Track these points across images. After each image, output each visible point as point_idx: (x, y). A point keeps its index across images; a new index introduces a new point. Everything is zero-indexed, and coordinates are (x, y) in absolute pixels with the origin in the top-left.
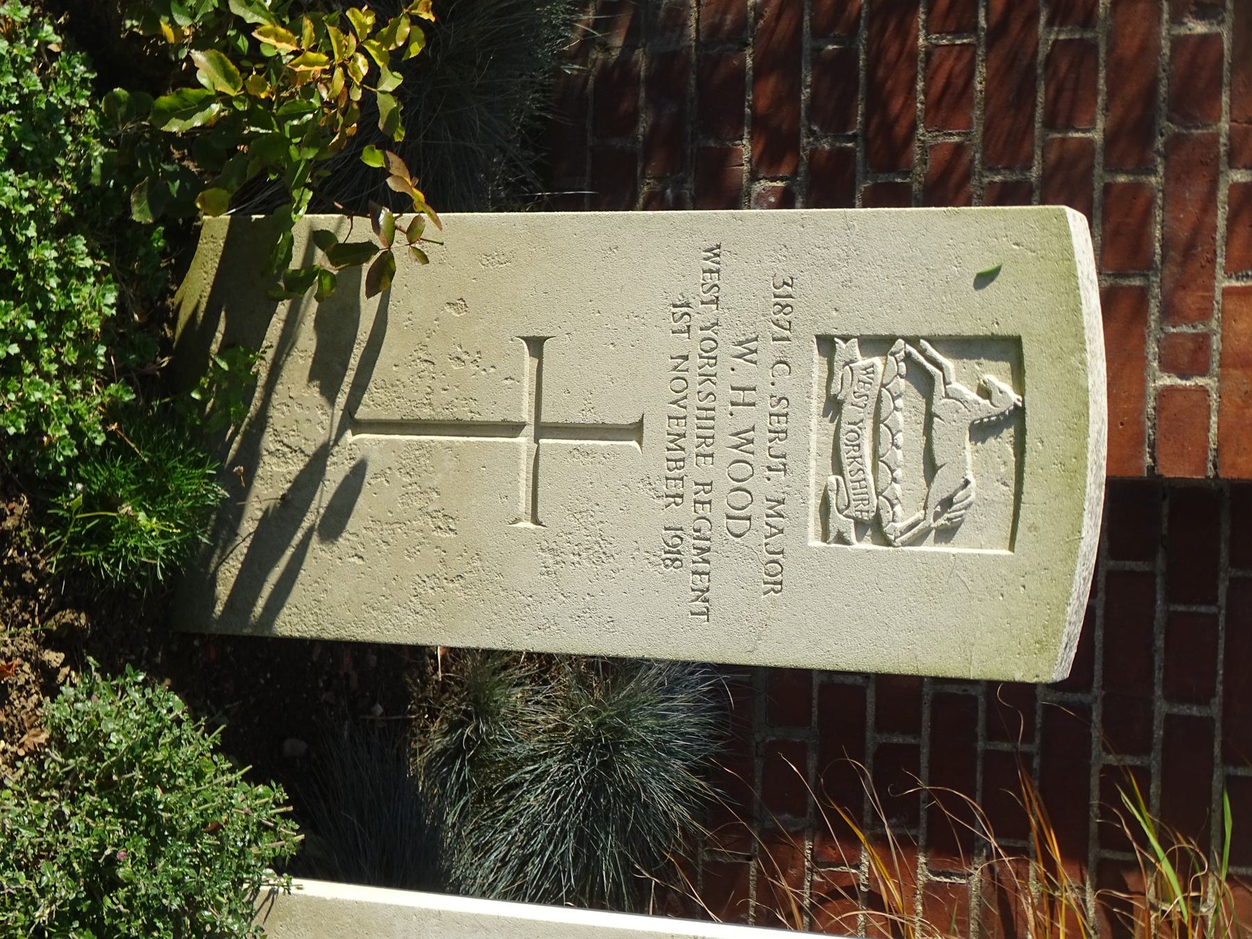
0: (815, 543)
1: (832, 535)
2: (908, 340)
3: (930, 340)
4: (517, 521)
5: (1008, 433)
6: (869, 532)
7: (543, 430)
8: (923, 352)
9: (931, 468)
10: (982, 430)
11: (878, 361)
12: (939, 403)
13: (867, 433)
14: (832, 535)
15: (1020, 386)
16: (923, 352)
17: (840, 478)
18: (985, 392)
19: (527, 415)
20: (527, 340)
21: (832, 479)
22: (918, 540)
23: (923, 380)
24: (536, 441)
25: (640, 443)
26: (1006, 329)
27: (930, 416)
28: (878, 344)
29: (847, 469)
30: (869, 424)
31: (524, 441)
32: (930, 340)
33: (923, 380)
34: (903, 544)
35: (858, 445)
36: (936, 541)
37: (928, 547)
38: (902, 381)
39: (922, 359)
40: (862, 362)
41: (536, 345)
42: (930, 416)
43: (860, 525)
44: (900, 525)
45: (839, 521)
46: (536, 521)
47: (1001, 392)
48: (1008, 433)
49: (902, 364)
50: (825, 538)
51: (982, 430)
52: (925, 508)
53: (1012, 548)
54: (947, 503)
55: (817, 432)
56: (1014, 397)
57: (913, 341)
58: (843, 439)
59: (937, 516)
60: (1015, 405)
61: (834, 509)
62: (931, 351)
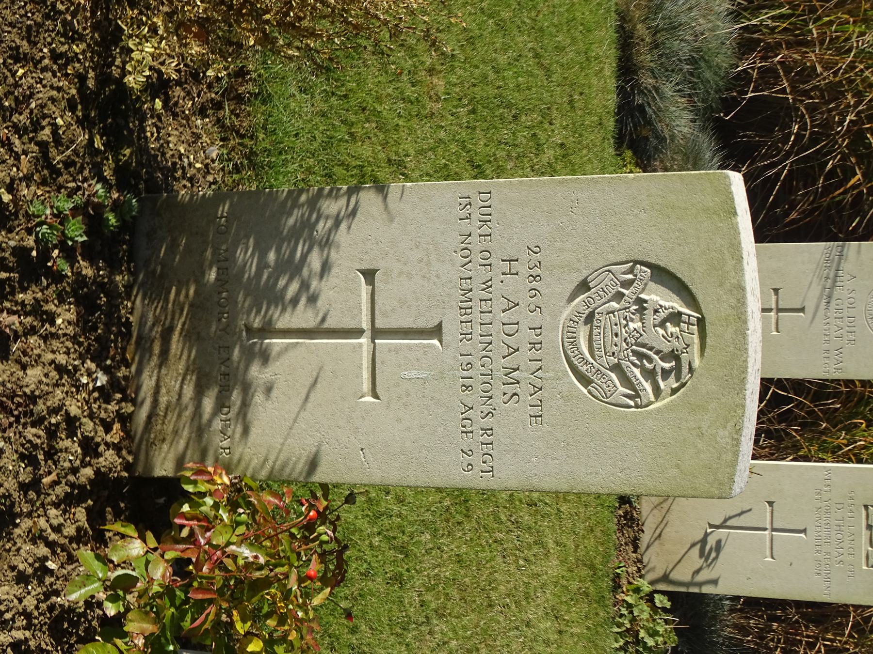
7: (774, 530)
14: (870, 565)
21: (870, 549)
25: (806, 535)
31: (766, 532)
41: (771, 503)
46: (772, 557)
50: (867, 566)
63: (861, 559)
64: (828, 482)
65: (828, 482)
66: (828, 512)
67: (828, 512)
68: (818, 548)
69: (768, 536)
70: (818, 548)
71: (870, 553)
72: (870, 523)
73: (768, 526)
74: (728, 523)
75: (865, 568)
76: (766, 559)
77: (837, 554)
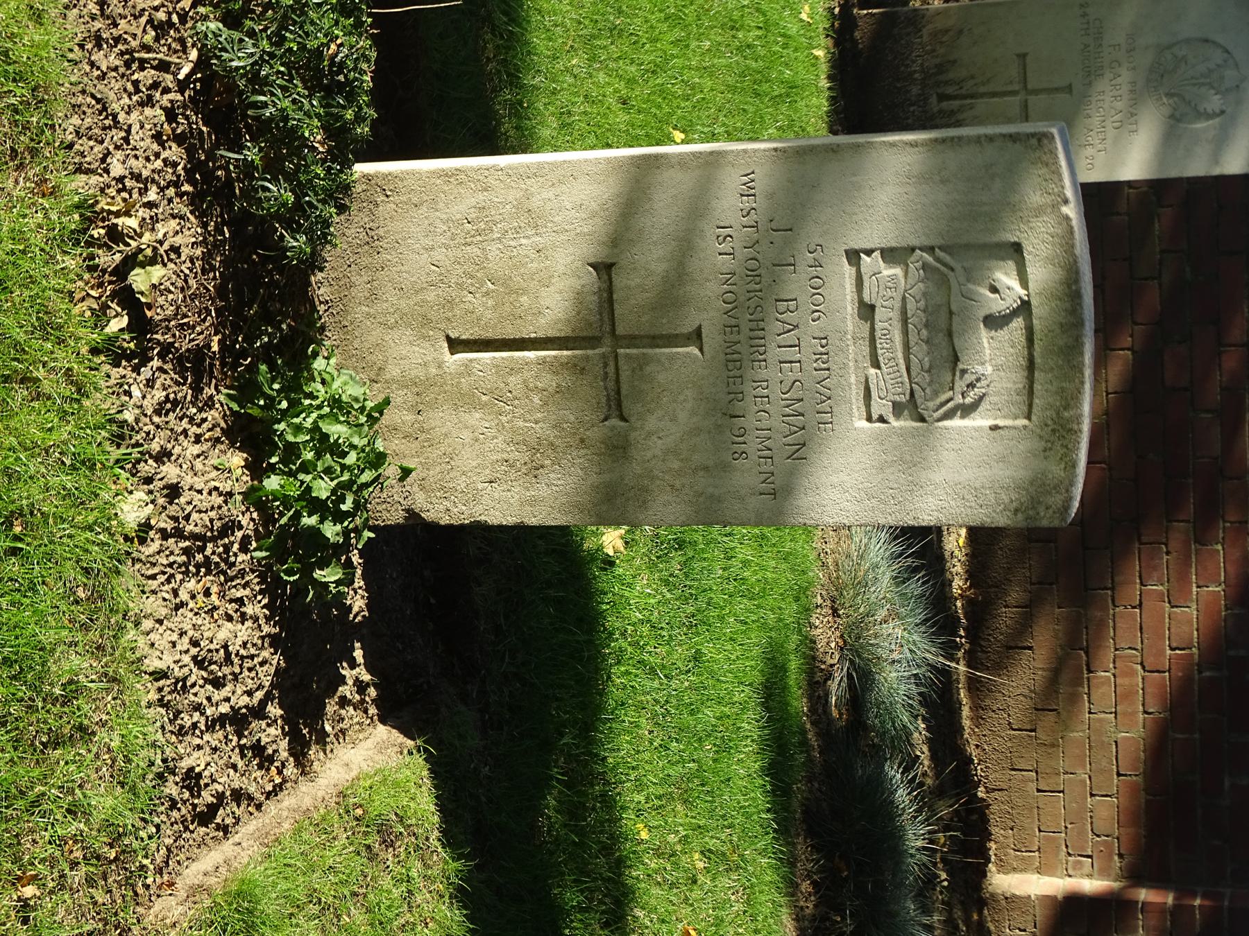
1: (875, 416)
6: (906, 412)
11: (898, 271)
14: (875, 416)
17: (878, 371)
21: (873, 371)
29: (882, 365)
36: (962, 417)
40: (888, 272)
46: (624, 419)
48: (1018, 323)
49: (921, 271)
50: (869, 419)
56: (1023, 292)
58: (878, 334)
61: (874, 394)
62: (947, 258)
75: (864, 424)
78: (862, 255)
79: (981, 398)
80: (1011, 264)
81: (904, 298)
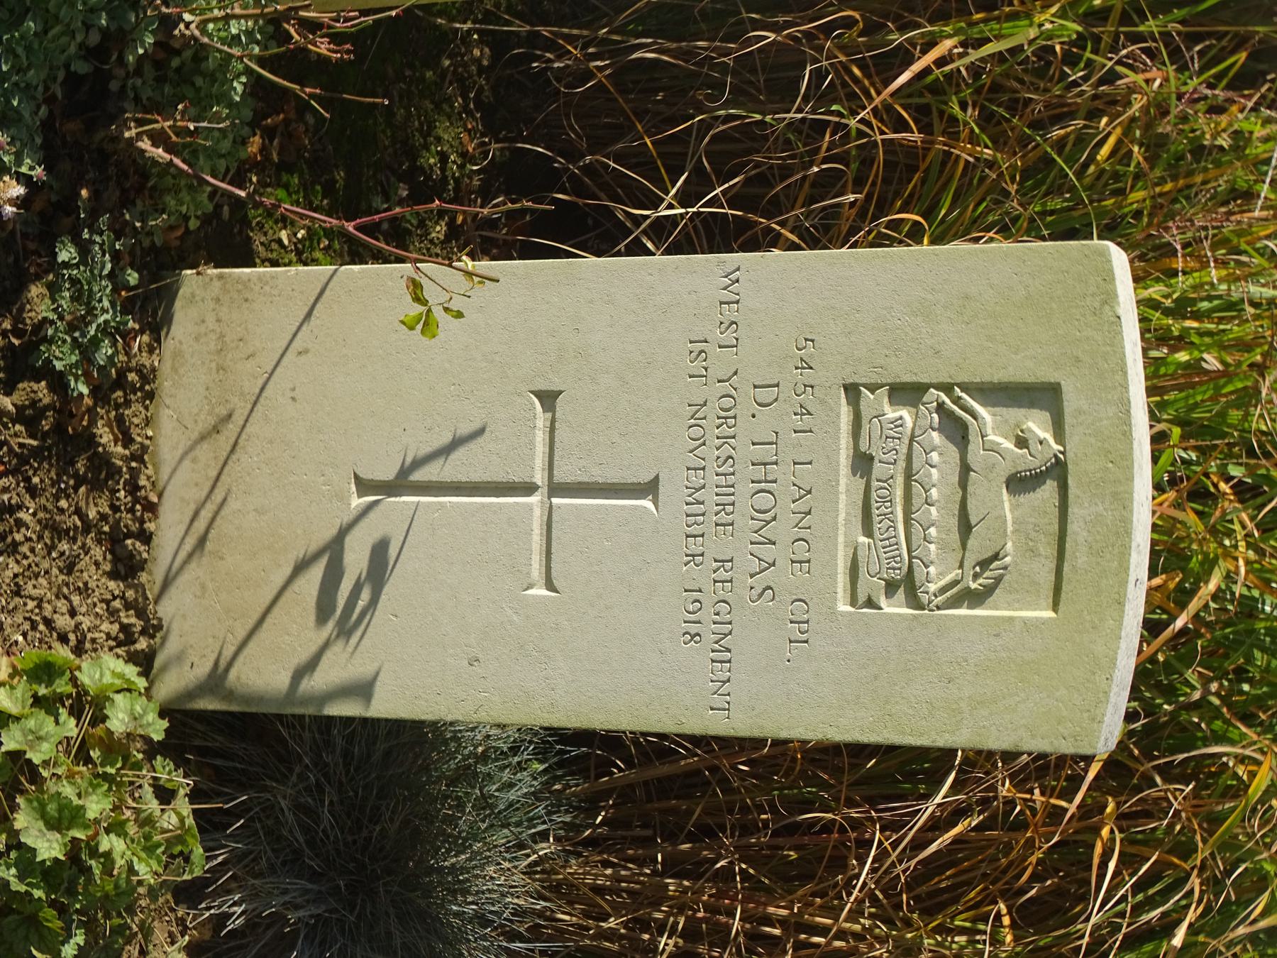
0: (843, 607)
1: (862, 598)
2: (939, 387)
3: (965, 387)
4: (530, 587)
5: (1050, 487)
7: (557, 489)
8: (957, 401)
9: (966, 527)
10: (1020, 483)
11: (905, 414)
12: (976, 453)
13: (899, 492)
14: (862, 598)
15: (1059, 434)
16: (957, 401)
17: (871, 541)
18: (1022, 442)
19: (539, 478)
20: (540, 395)
21: (863, 540)
22: (955, 603)
23: (957, 431)
24: (549, 498)
26: (1047, 374)
27: (965, 469)
28: (908, 393)
30: (900, 480)
31: (534, 499)
32: (965, 387)
33: (957, 431)
34: (938, 608)
35: (891, 501)
37: (963, 611)
38: (935, 434)
39: (955, 408)
40: (891, 413)
41: (548, 399)
42: (965, 469)
43: (891, 588)
44: (933, 587)
45: (871, 584)
46: (550, 586)
47: (1041, 443)
48: (1050, 487)
49: (935, 416)
50: (853, 603)
51: (1020, 483)
52: (961, 566)
53: (1055, 609)
54: (984, 564)
55: (847, 486)
57: (947, 388)
58: (874, 495)
59: (976, 576)
60: (1055, 456)
61: (863, 570)
63: (833, 576)
64: (729, 313)
65: (729, 313)
66: (727, 416)
67: (727, 416)
68: (694, 546)
69: (537, 512)
70: (694, 546)
71: (862, 554)
72: (863, 447)
73: (539, 478)
74: (418, 476)
76: (530, 592)
77: (755, 565)
78: (862, 388)
79: (998, 580)
80: (1046, 415)
81: (910, 446)
